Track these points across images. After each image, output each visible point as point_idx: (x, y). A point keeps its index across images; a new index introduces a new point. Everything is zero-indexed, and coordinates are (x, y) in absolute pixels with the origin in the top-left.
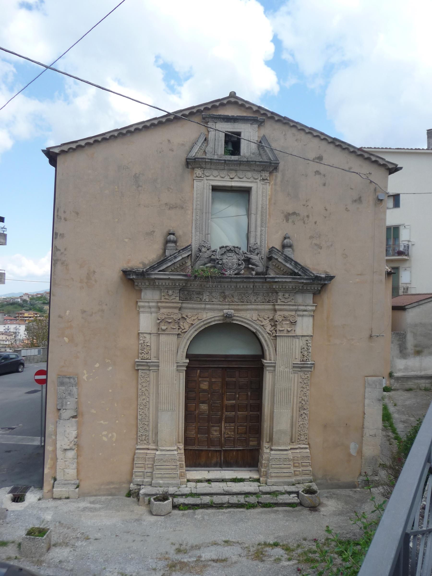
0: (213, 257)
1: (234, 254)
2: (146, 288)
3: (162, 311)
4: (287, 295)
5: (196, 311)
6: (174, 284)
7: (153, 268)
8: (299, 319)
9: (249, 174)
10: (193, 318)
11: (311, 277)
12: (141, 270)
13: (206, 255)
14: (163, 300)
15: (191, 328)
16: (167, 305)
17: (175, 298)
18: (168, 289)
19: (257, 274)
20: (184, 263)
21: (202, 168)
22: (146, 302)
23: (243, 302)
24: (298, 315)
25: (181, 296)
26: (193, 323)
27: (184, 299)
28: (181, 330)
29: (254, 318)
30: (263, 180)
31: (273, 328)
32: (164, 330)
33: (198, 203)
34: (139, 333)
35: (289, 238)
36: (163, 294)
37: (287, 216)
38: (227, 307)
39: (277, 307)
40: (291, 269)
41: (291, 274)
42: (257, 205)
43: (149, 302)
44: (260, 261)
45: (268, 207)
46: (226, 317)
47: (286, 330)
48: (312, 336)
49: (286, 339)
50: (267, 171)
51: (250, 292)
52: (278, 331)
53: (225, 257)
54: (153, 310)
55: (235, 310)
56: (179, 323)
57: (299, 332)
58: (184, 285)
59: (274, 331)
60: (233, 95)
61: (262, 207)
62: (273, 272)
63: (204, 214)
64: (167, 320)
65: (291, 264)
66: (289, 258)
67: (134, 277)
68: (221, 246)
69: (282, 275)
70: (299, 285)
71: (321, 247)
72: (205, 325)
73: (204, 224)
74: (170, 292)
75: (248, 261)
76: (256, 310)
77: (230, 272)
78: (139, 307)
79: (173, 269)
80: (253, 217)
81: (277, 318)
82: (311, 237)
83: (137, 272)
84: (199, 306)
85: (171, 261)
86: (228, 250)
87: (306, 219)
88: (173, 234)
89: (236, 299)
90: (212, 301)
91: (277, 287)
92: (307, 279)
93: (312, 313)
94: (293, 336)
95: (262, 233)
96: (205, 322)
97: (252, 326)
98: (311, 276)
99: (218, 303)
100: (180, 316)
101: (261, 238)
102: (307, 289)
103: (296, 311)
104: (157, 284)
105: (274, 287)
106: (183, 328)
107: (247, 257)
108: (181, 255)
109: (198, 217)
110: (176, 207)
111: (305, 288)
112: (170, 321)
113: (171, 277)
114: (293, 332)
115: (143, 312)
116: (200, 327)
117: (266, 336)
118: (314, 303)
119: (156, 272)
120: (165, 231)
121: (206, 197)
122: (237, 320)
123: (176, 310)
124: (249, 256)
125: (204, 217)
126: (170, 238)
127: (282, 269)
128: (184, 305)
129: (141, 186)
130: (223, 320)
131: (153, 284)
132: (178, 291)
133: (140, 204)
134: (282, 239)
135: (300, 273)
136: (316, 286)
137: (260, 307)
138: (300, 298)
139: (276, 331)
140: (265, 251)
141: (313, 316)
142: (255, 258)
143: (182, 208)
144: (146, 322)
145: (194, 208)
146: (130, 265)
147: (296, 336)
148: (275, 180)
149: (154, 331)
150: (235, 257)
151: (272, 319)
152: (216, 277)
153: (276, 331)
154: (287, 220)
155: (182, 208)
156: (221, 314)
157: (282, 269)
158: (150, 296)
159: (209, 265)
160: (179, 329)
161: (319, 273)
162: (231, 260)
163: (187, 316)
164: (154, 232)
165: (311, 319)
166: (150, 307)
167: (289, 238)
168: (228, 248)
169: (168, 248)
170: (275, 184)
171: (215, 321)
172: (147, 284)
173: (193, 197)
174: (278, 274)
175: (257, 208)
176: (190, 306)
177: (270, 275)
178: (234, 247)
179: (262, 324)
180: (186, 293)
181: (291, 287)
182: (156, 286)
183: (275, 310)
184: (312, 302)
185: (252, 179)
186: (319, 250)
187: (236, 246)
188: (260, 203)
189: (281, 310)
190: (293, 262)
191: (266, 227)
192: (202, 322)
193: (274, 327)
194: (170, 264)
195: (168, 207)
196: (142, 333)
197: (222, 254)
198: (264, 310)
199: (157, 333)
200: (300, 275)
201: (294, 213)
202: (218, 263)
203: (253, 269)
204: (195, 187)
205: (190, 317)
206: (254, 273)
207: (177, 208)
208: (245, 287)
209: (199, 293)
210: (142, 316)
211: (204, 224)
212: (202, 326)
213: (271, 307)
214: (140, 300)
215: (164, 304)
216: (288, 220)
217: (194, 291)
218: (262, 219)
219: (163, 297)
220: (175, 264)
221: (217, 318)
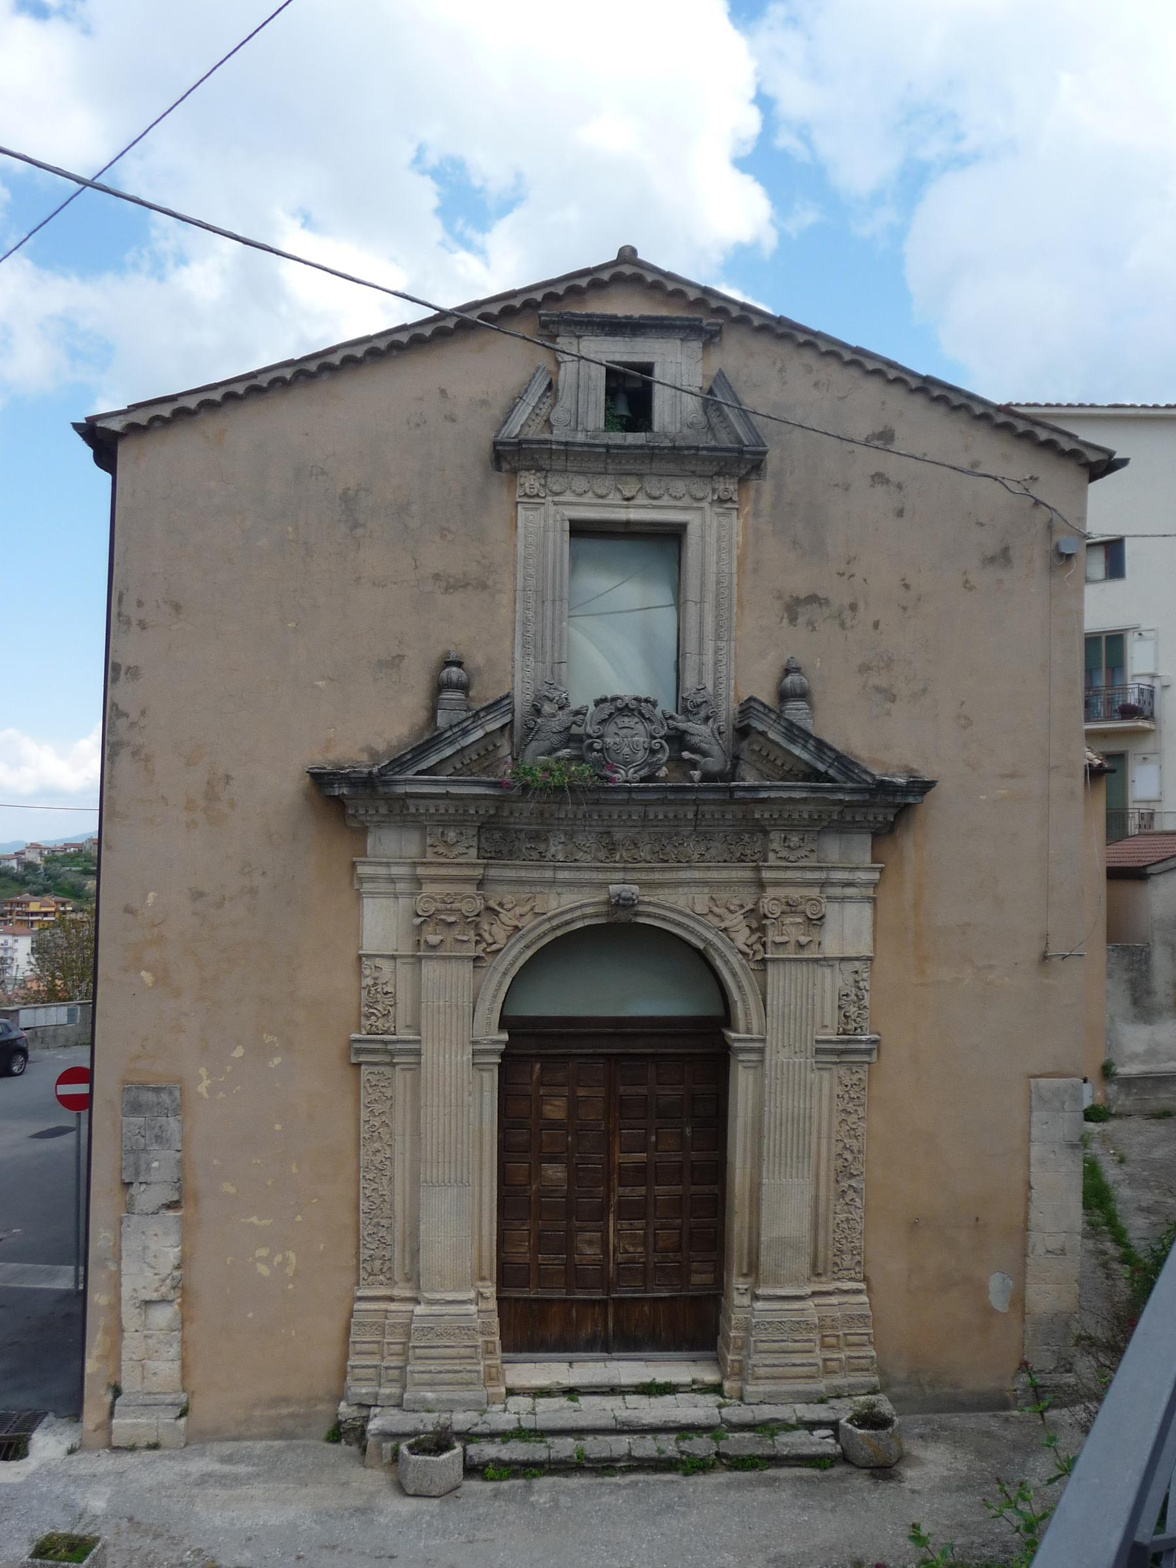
0: (575, 730)
1: (636, 720)
2: (379, 825)
3: (429, 889)
4: (795, 840)
5: (527, 889)
6: (461, 812)
7: (399, 764)
8: (832, 911)
9: (679, 486)
10: (518, 910)
12: (366, 770)
13: (555, 725)
14: (430, 857)
15: (513, 940)
16: (443, 871)
17: (465, 851)
18: (444, 824)
19: (707, 777)
20: (491, 748)
21: (539, 469)
22: (380, 864)
23: (667, 861)
24: (828, 898)
25: (485, 845)
26: (520, 925)
27: (493, 855)
28: (484, 945)
29: (701, 908)
30: (721, 501)
31: (755, 937)
32: (434, 947)
33: (531, 571)
34: (360, 957)
35: (798, 670)
36: (429, 841)
37: (793, 608)
38: (619, 876)
39: (766, 875)
40: (807, 763)
41: (806, 778)
42: (703, 575)
43: (388, 864)
44: (713, 741)
45: (735, 580)
46: (617, 904)
47: (793, 943)
48: (870, 959)
49: (793, 969)
50: (732, 476)
51: (686, 830)
52: (769, 944)
53: (611, 728)
54: (401, 887)
55: (642, 884)
56: (477, 925)
57: (831, 948)
58: (492, 812)
59: (758, 947)
60: (627, 255)
61: (718, 583)
62: (754, 772)
63: (548, 604)
64: (443, 917)
65: (805, 747)
66: (799, 728)
67: (345, 791)
68: (598, 697)
69: (780, 780)
71: (895, 696)
72: (554, 929)
73: (548, 632)
74: (452, 835)
75: (678, 739)
76: (705, 883)
77: (626, 772)
78: (361, 880)
79: (459, 766)
80: (692, 610)
81: (769, 905)
82: (865, 668)
83: (354, 775)
84: (535, 874)
85: (451, 743)
86: (618, 709)
87: (847, 613)
88: (459, 664)
89: (644, 853)
90: (576, 860)
91: (767, 815)
92: (853, 791)
93: (870, 892)
94: (816, 961)
95: (720, 658)
96: (555, 923)
97: (692, 931)
98: (867, 782)
99: (593, 865)
100: (479, 905)
101: (716, 671)
102: (854, 822)
103: (823, 884)
104: (412, 810)
105: (757, 816)
106: (490, 941)
107: (676, 729)
108: (482, 726)
109: (531, 614)
111: (848, 818)
112: (451, 919)
113: (454, 790)
114: (814, 946)
115: (373, 895)
116: (540, 937)
117: (735, 960)
118: (875, 860)
119: (409, 775)
120: (436, 654)
121: (555, 555)
122: (649, 915)
123: (468, 887)
124: (682, 726)
125: (549, 613)
126: (449, 679)
127: (779, 762)
128: (493, 873)
129: (364, 525)
130: (608, 914)
131: (402, 813)
132: (472, 832)
134: (776, 672)
135: (831, 772)
136: (881, 810)
137: (714, 875)
138: (832, 848)
139: (764, 945)
140: (728, 710)
141: (874, 899)
142: (700, 731)
143: (484, 587)
144: (382, 923)
145: (520, 586)
146: (331, 756)
147: (825, 959)
148: (757, 502)
149: (406, 949)
150: (640, 727)
151: (752, 910)
152: (586, 790)
153: (764, 945)
154: (793, 620)
155: (484, 587)
156: (602, 897)
157: (779, 762)
158: (391, 846)
159: (564, 752)
160: (477, 942)
161: (891, 771)
162: (630, 739)
163: (501, 905)
164: (401, 657)
165: (867, 910)
166: (392, 880)
167: (798, 670)
168: (619, 704)
169: (445, 704)
170: (756, 514)
171: (584, 917)
172: (383, 810)
173: (515, 555)
175: (703, 584)
176: (511, 874)
177: (744, 780)
178: (637, 699)
179: (723, 925)
180: (497, 836)
181: (806, 816)
182: (409, 818)
183: (761, 885)
184: (868, 858)
185: (686, 501)
186: (888, 705)
187: (643, 696)
188: (712, 569)
189: (777, 883)
190: (811, 742)
191: (729, 640)
192: (545, 920)
193: (759, 934)
194: (448, 752)
195: (443, 584)
196: (368, 956)
197: (603, 722)
198: (727, 884)
199: (413, 956)
200: (832, 780)
201: (813, 599)
202: (591, 748)
203: (694, 765)
204: (520, 524)
205: (510, 906)
206: (696, 774)
208: (671, 816)
209: (536, 837)
210: (369, 904)
211: (548, 632)
212: (545, 934)
213: (748, 874)
214: (363, 859)
215: (432, 871)
217: (521, 831)
218: (718, 617)
219: (429, 849)
220: (466, 752)
221: (589, 910)
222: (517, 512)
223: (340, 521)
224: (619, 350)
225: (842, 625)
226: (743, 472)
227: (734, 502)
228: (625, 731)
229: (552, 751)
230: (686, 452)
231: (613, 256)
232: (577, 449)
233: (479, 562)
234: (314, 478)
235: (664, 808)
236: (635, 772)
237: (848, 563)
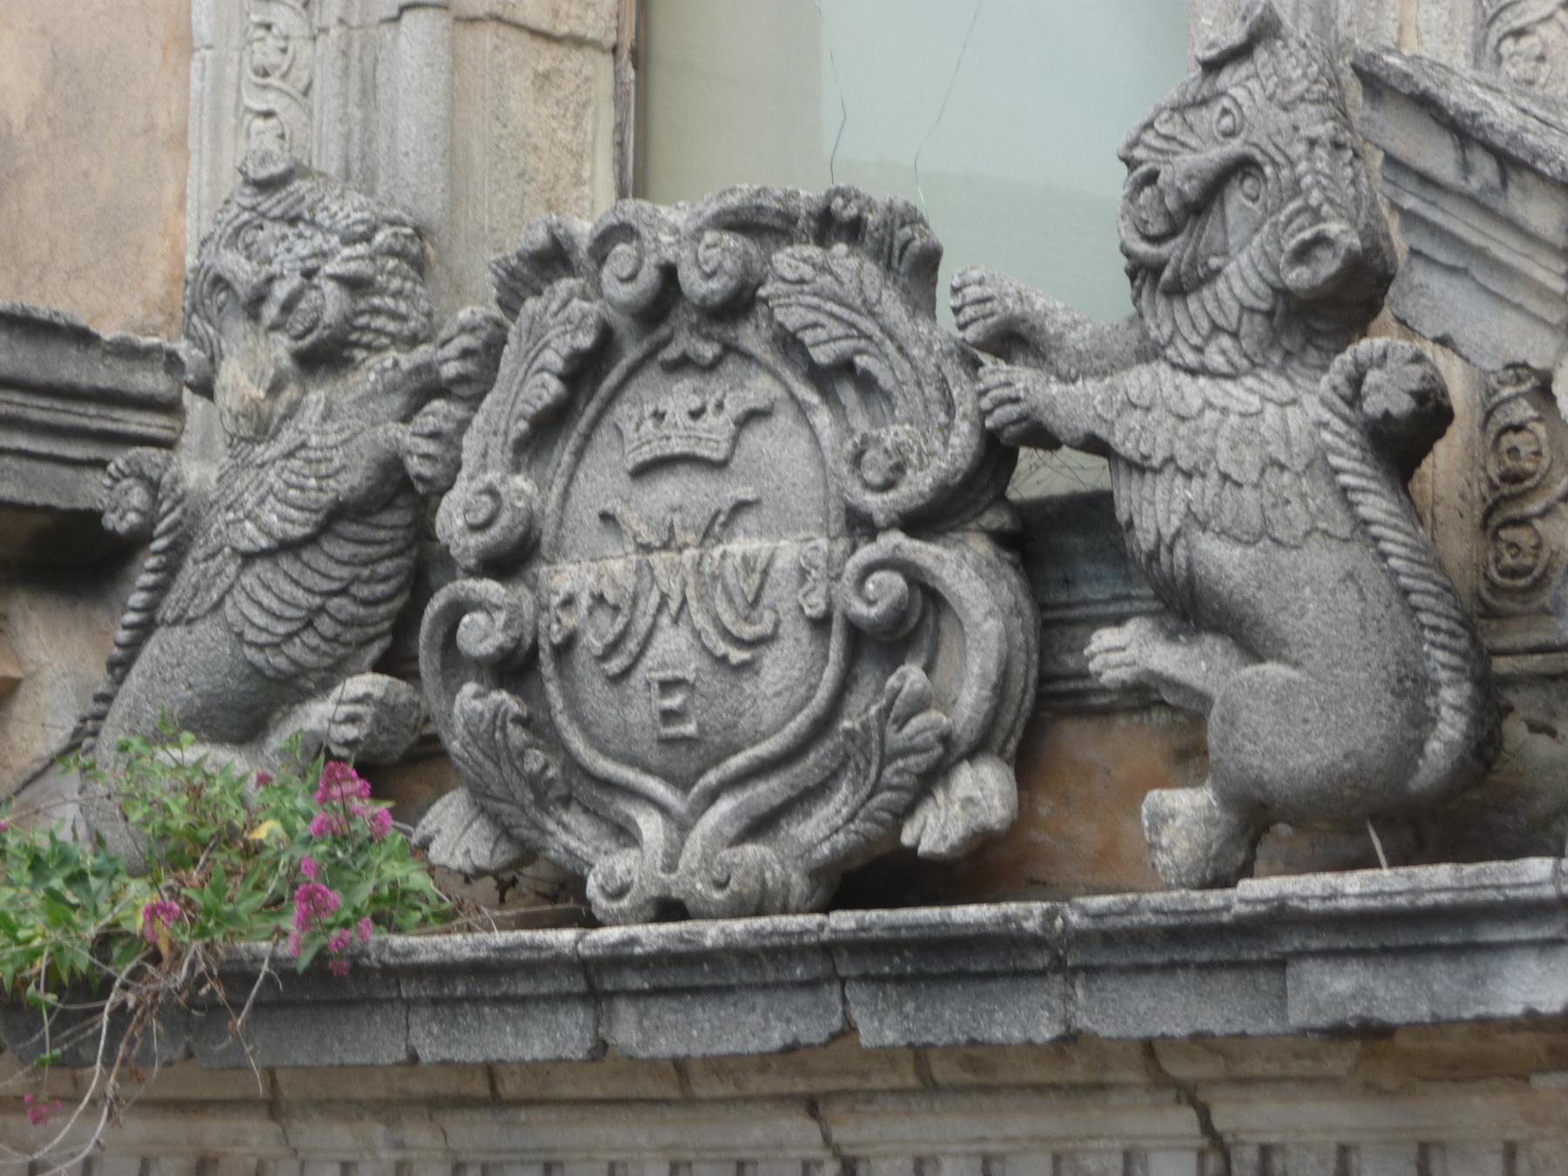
1: (760, 389)
19: (1258, 823)
162: (702, 553)
206: (1183, 813)
229: (244, 713)
235: (1051, 1122)
236: (760, 826)
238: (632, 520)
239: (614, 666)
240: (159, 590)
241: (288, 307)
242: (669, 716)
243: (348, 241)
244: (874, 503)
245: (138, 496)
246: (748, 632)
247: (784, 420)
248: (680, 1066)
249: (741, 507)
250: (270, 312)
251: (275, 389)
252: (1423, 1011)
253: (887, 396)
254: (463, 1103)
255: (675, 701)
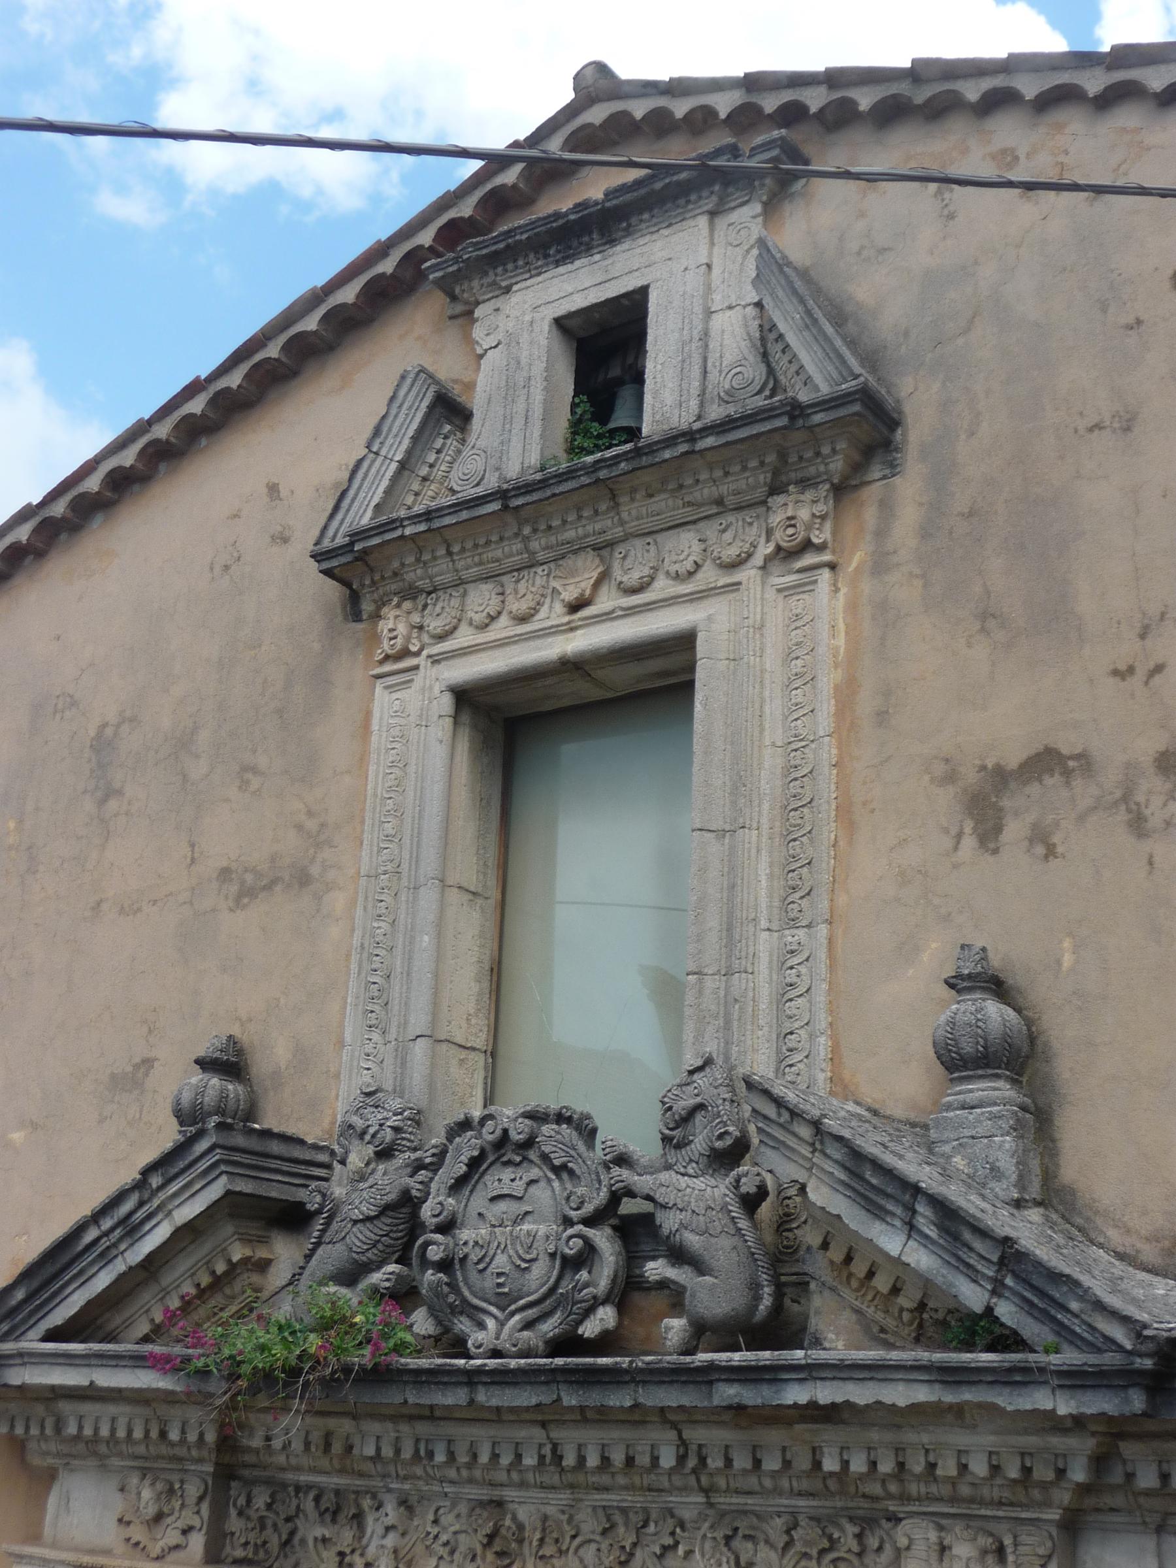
1: (535, 1173)
9: (685, 546)
11: (1110, 1359)
19: (703, 1332)
21: (411, 593)
30: (785, 555)
37: (986, 802)
50: (805, 483)
60: (596, 83)
70: (1071, 1442)
85: (106, 1258)
91: (858, 1465)
92: (1075, 1380)
98: (1120, 1348)
110: (268, 887)
129: (119, 793)
133: (99, 903)
135: (1005, 1311)
143: (303, 879)
148: (881, 533)
154: (989, 835)
155: (303, 879)
162: (514, 1228)
164: (148, 1063)
170: (880, 565)
174: (881, 1337)
177: (817, 1343)
180: (261, 1499)
185: (709, 576)
194: (103, 1280)
195: (234, 888)
200: (1008, 1341)
201: (1046, 762)
204: (375, 727)
206: (675, 1327)
207: (278, 888)
216: (998, 829)
222: (371, 699)
223: (85, 792)
224: (579, 285)
225: (1138, 825)
226: (837, 465)
227: (822, 548)
228: (502, 1206)
229: (350, 1276)
230: (667, 454)
231: (567, 95)
232: (448, 521)
233: (299, 827)
234: (58, 716)
235: (627, 1434)
236: (528, 1325)
237: (1143, 636)
238: (489, 1216)
239: (481, 1267)
240: (323, 1231)
241: (374, 1136)
242: (499, 1285)
243: (395, 1115)
244: (573, 1214)
245: (318, 1199)
246: (528, 1257)
247: (543, 1184)
248: (498, 1409)
249: (527, 1213)
250: (368, 1137)
251: (367, 1164)
252: (759, 1401)
253: (579, 1177)
254: (421, 1418)
255: (501, 1280)
